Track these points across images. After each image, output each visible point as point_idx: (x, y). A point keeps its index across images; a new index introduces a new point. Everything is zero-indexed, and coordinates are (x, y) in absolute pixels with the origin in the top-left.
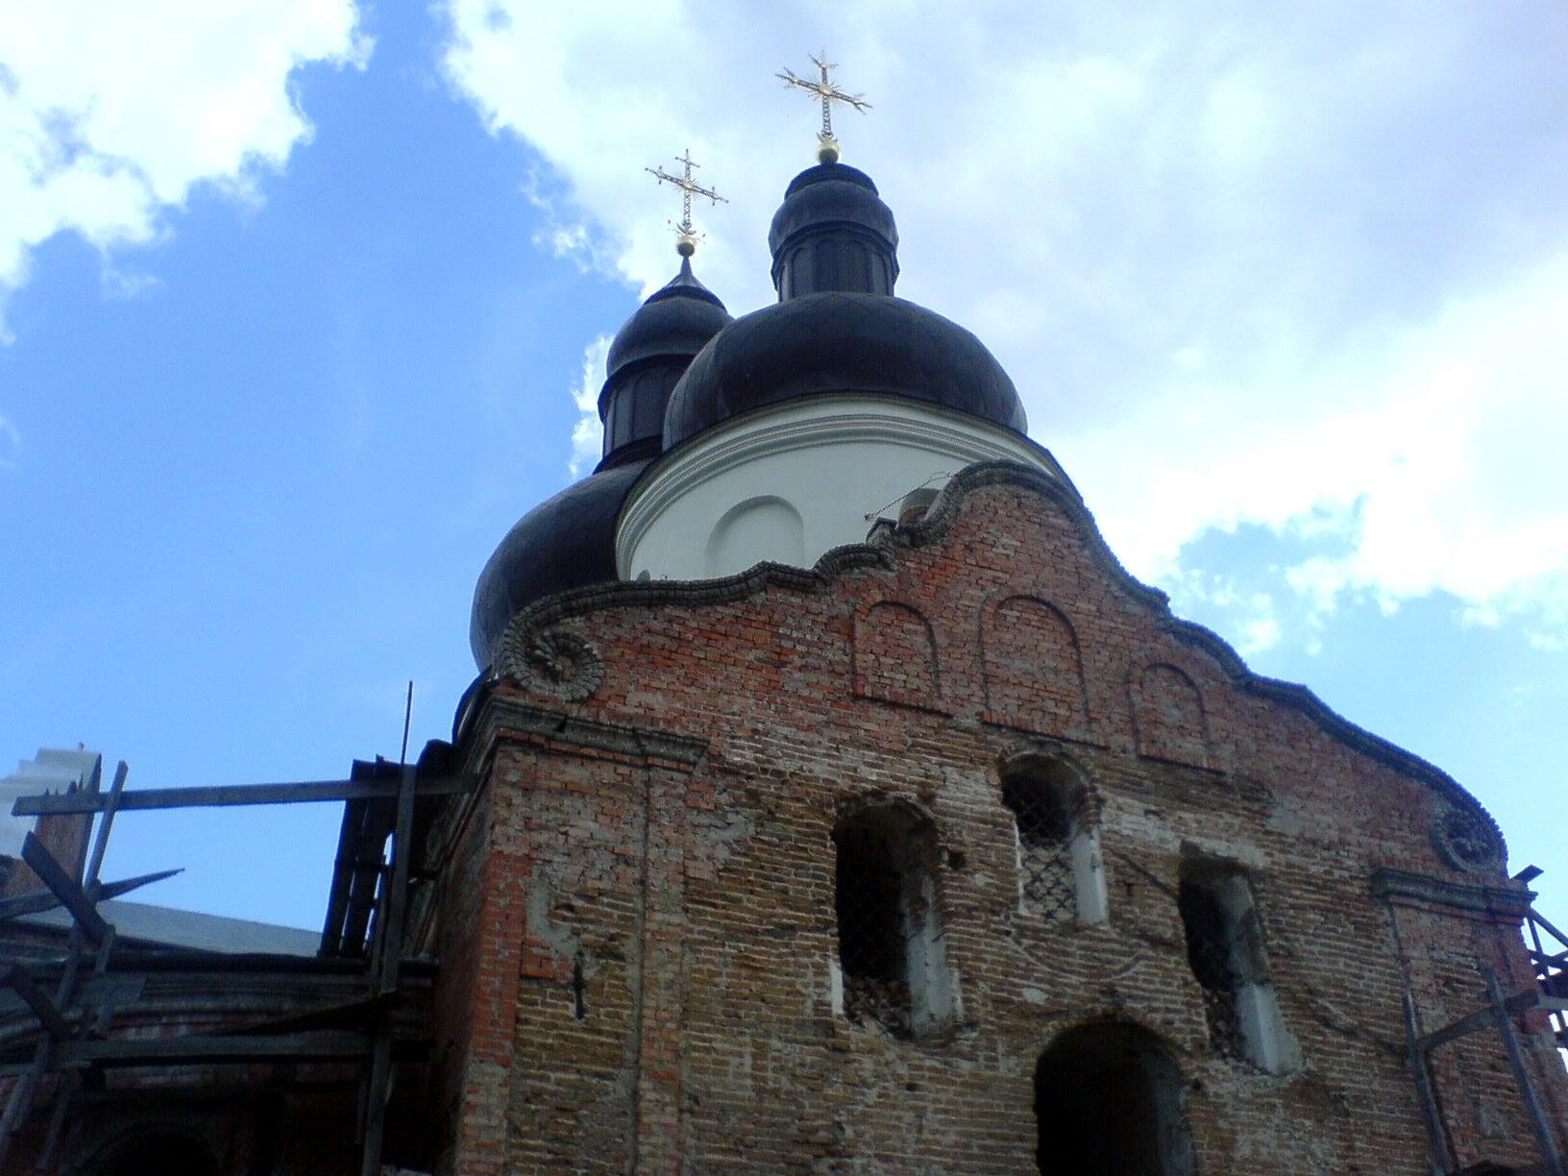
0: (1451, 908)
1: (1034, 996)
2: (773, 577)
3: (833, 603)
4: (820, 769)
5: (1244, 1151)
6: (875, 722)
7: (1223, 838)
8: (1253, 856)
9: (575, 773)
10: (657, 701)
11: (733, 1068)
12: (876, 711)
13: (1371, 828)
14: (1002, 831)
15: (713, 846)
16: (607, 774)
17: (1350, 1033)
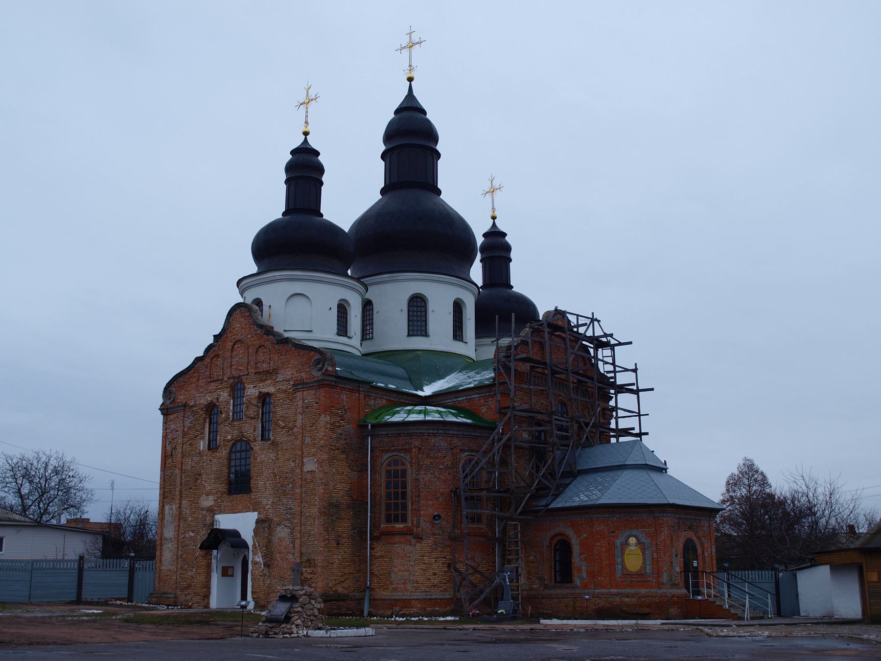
0: (311, 388)
1: (229, 437)
2: (198, 360)
3: (208, 360)
4: (202, 402)
5: (259, 459)
6: (213, 386)
7: (269, 388)
8: (271, 390)
9: (172, 416)
10: (182, 397)
11: (189, 464)
12: (212, 384)
13: (299, 371)
14: (228, 403)
15: (187, 423)
16: (175, 415)
17: (283, 428)
